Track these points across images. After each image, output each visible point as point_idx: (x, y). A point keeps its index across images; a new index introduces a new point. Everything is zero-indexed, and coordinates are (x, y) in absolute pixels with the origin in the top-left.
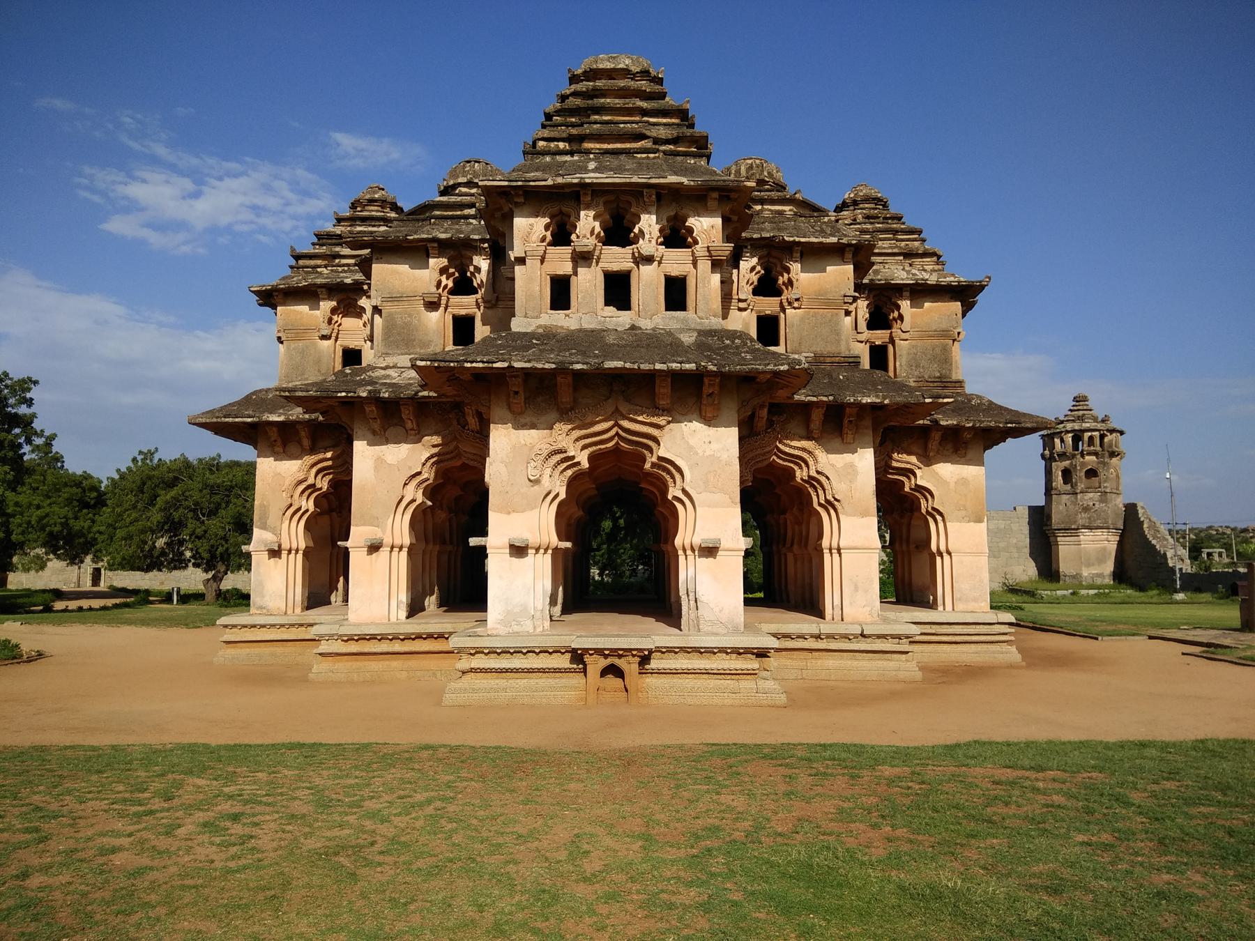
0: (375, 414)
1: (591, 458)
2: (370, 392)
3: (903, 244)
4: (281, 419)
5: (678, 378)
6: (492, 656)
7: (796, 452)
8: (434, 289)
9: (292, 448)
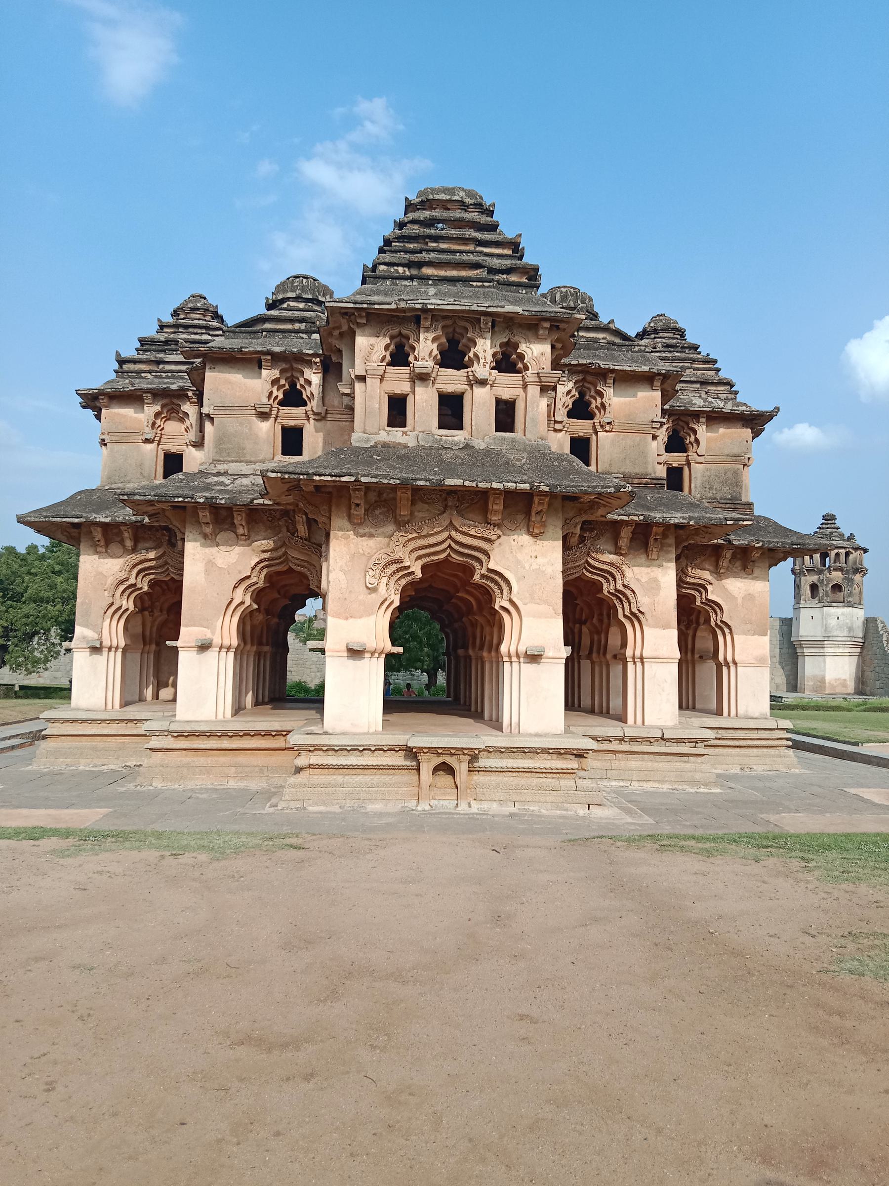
0: (208, 520)
1: (423, 568)
2: (206, 498)
3: (699, 372)
4: (108, 520)
5: (509, 495)
6: (330, 753)
7: (604, 567)
8: (265, 400)
9: (114, 548)
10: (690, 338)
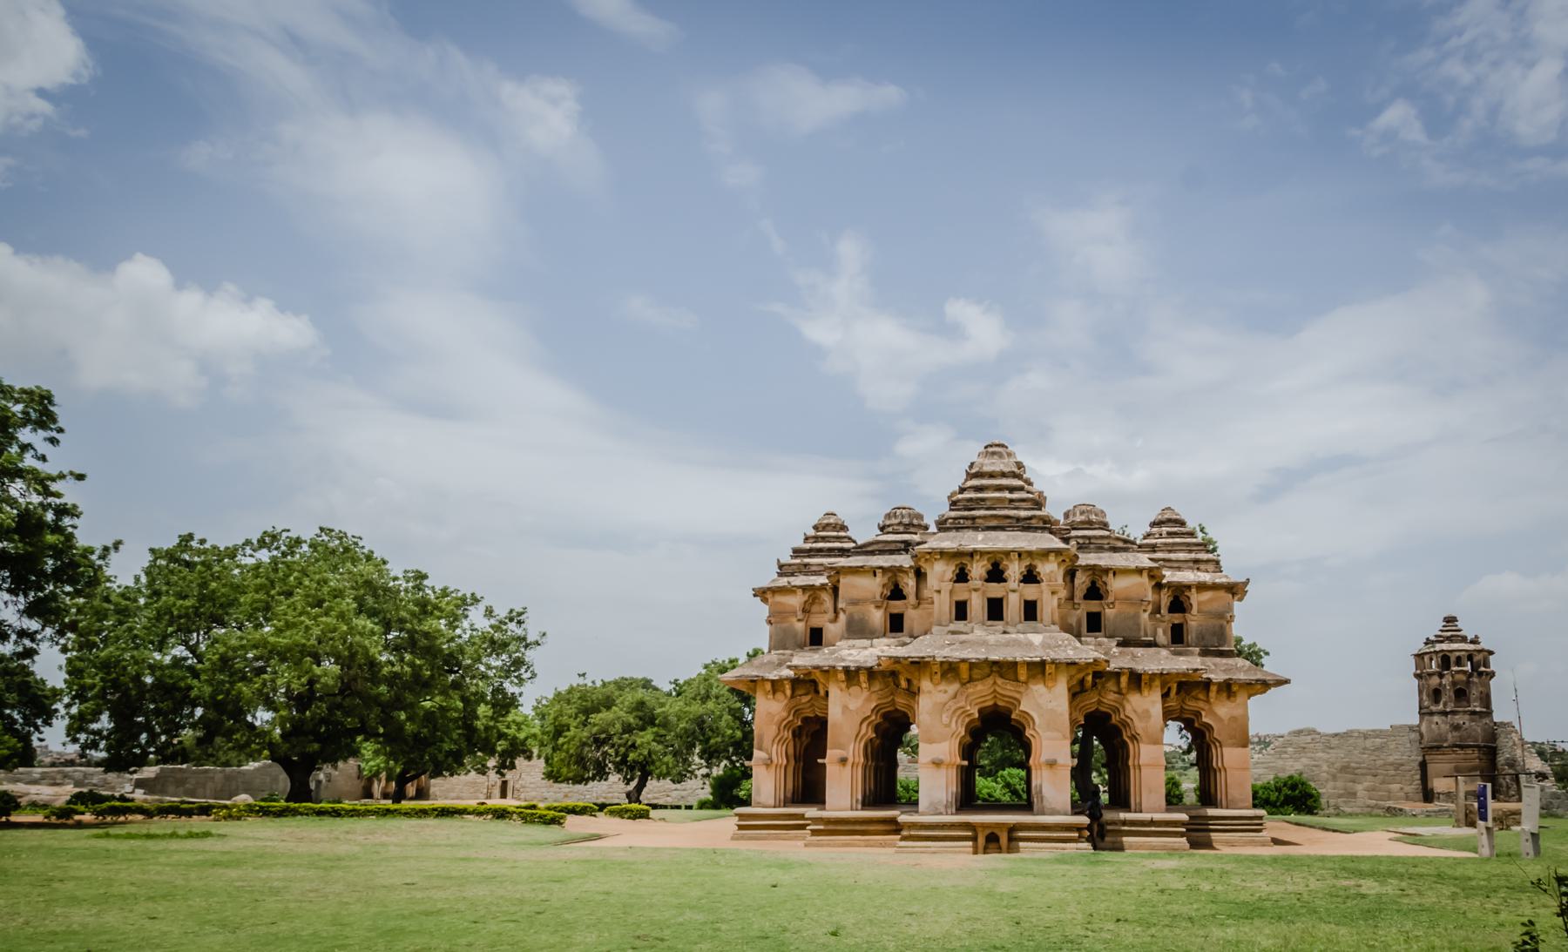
1: (980, 711)
9: (779, 695)
10: (1191, 524)
